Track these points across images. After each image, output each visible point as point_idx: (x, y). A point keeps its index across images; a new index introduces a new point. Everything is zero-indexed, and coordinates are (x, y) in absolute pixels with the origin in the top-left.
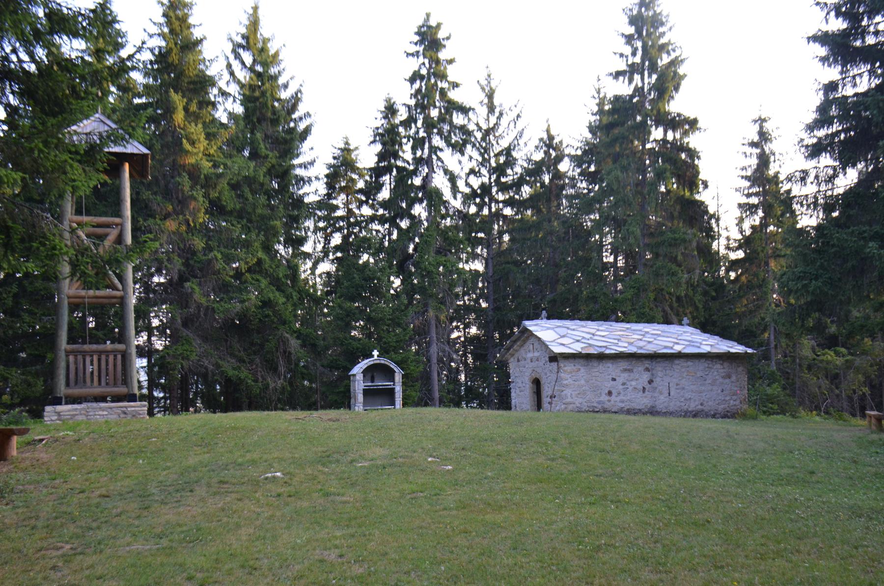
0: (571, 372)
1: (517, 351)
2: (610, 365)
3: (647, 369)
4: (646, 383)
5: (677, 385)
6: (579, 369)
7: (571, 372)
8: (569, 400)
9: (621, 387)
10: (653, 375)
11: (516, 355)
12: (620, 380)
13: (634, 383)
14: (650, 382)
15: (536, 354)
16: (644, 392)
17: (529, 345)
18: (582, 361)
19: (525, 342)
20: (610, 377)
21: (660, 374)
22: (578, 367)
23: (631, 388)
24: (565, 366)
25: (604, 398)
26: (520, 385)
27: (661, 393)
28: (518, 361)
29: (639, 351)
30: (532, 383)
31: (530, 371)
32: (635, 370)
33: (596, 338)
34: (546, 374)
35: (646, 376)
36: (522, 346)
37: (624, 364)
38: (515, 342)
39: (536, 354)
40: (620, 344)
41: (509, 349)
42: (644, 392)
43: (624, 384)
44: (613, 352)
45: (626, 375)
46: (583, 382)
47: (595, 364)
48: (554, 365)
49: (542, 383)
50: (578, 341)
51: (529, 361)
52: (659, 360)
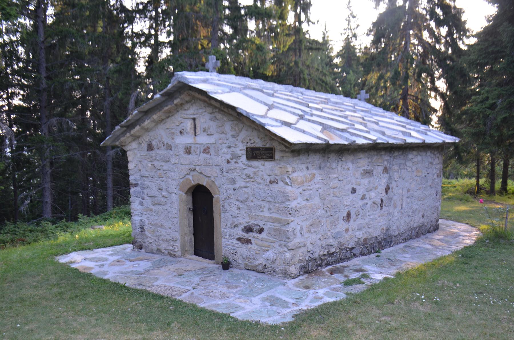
0: (302, 183)
1: (147, 130)
2: (350, 165)
3: (386, 170)
4: (384, 194)
5: (409, 191)
6: (314, 175)
7: (302, 183)
8: (298, 240)
9: (361, 203)
10: (390, 178)
11: (146, 138)
12: (360, 191)
13: (373, 194)
14: (387, 190)
15: (203, 139)
16: (382, 208)
17: (183, 119)
18: (316, 159)
19: (169, 114)
20: (350, 187)
21: (396, 176)
22: (312, 171)
23: (370, 203)
24: (294, 171)
25: (342, 226)
26: (154, 192)
27: (395, 207)
28: (150, 148)
29: (391, 141)
30: (186, 193)
31: (184, 170)
32: (375, 172)
33: (301, 113)
34: (233, 182)
35: (383, 182)
36: (161, 121)
37: (364, 162)
38: (147, 113)
39: (203, 139)
40: (302, 125)
41: (130, 126)
42: (382, 208)
43: (363, 198)
44: (365, 142)
45: (365, 181)
46: (317, 201)
47: (334, 165)
48: (264, 168)
49: (218, 197)
50: (301, 117)
51: (182, 151)
52: (396, 153)
